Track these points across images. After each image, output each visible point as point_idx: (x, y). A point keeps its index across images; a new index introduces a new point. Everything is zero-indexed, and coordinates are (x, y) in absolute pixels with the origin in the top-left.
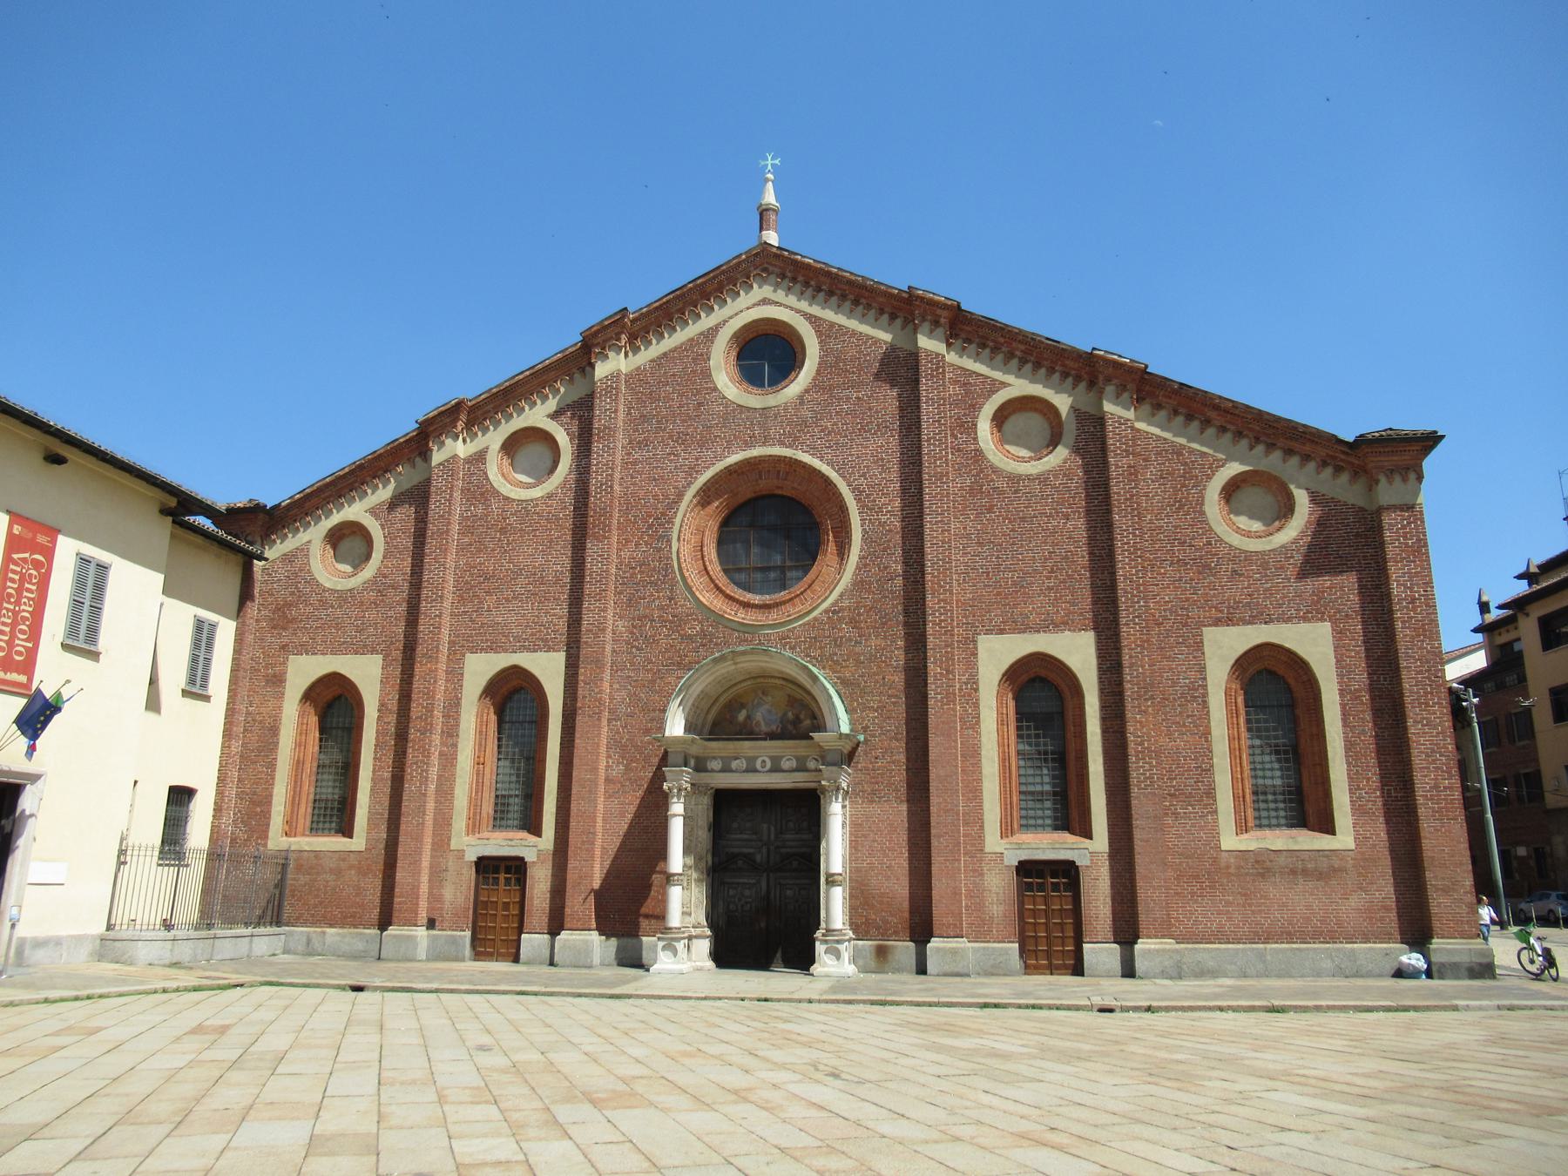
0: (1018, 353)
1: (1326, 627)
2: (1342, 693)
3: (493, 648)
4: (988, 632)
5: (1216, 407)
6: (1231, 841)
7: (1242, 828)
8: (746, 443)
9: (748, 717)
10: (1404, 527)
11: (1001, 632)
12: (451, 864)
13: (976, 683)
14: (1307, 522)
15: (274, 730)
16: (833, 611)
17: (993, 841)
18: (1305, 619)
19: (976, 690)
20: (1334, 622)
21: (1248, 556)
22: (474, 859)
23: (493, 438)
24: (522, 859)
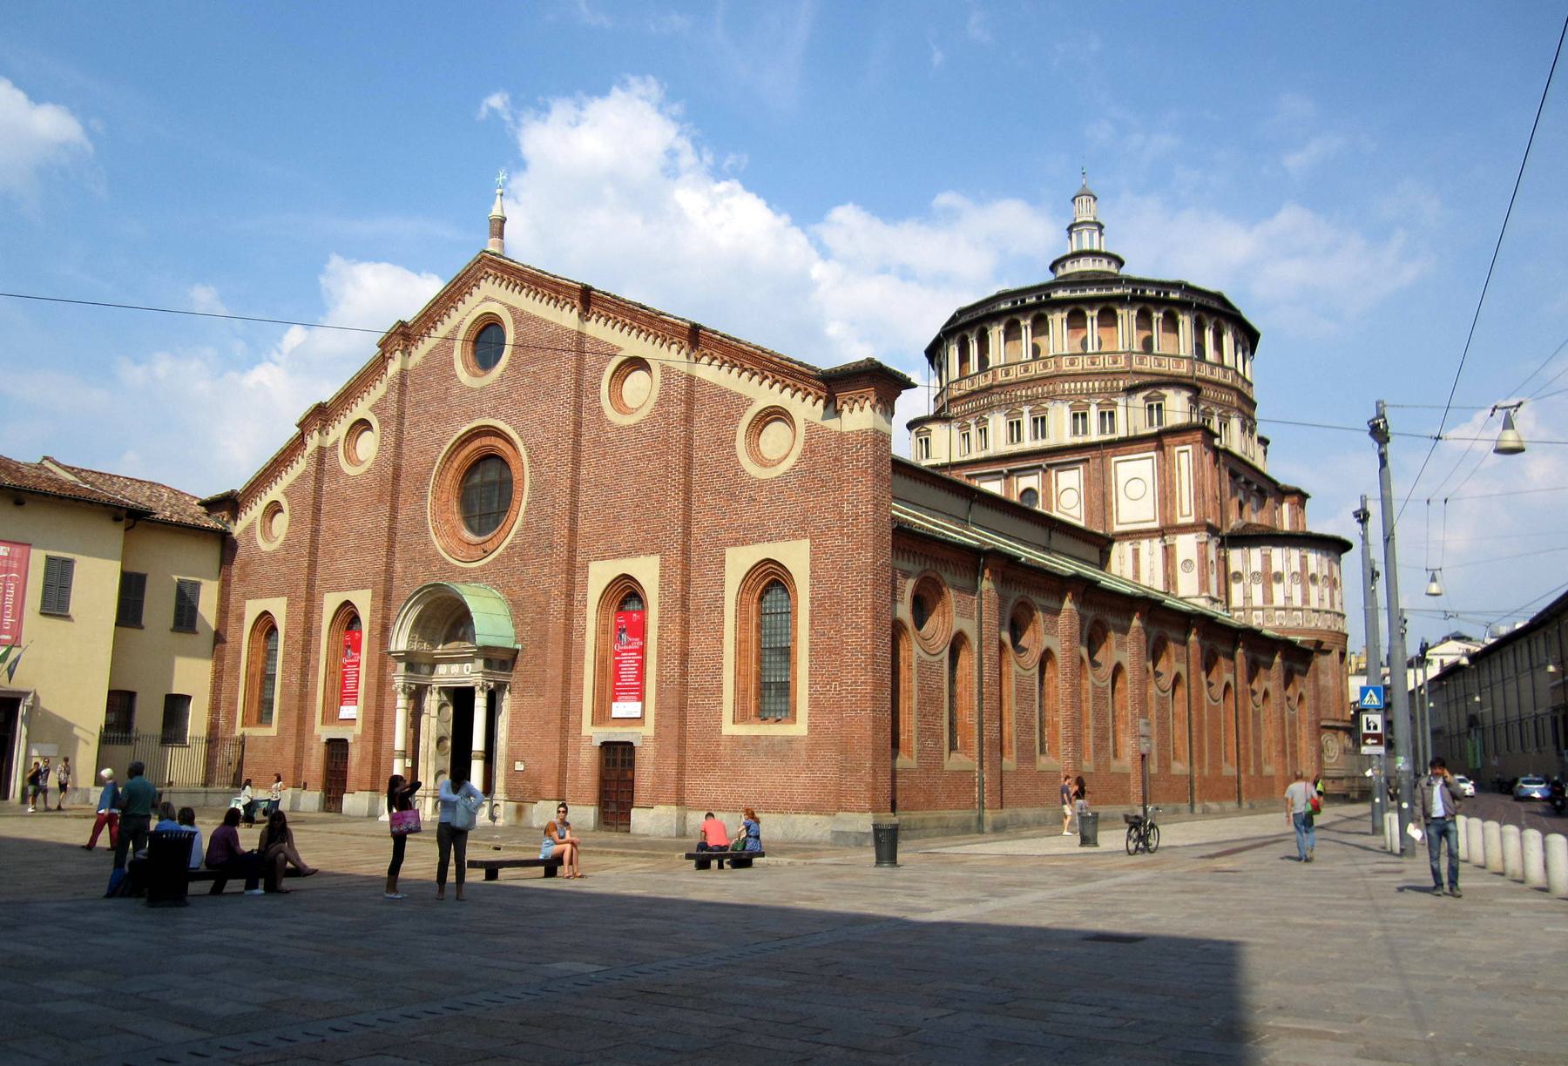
0: (628, 321)
1: (806, 543)
2: (812, 603)
3: (338, 589)
4: (596, 559)
5: (744, 352)
6: (729, 728)
7: (741, 717)
8: (470, 416)
9: (464, 633)
10: (857, 451)
11: (604, 558)
12: (315, 746)
13: (586, 601)
14: (803, 449)
15: (239, 653)
16: (511, 547)
17: (587, 729)
18: (794, 537)
19: (586, 606)
20: (812, 539)
21: (761, 484)
22: (325, 741)
23: (339, 430)
24: (346, 740)
